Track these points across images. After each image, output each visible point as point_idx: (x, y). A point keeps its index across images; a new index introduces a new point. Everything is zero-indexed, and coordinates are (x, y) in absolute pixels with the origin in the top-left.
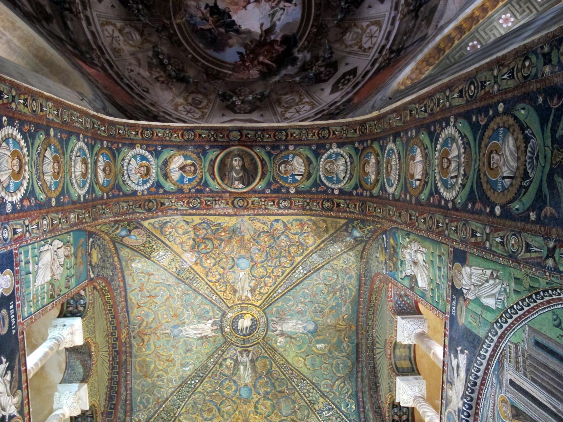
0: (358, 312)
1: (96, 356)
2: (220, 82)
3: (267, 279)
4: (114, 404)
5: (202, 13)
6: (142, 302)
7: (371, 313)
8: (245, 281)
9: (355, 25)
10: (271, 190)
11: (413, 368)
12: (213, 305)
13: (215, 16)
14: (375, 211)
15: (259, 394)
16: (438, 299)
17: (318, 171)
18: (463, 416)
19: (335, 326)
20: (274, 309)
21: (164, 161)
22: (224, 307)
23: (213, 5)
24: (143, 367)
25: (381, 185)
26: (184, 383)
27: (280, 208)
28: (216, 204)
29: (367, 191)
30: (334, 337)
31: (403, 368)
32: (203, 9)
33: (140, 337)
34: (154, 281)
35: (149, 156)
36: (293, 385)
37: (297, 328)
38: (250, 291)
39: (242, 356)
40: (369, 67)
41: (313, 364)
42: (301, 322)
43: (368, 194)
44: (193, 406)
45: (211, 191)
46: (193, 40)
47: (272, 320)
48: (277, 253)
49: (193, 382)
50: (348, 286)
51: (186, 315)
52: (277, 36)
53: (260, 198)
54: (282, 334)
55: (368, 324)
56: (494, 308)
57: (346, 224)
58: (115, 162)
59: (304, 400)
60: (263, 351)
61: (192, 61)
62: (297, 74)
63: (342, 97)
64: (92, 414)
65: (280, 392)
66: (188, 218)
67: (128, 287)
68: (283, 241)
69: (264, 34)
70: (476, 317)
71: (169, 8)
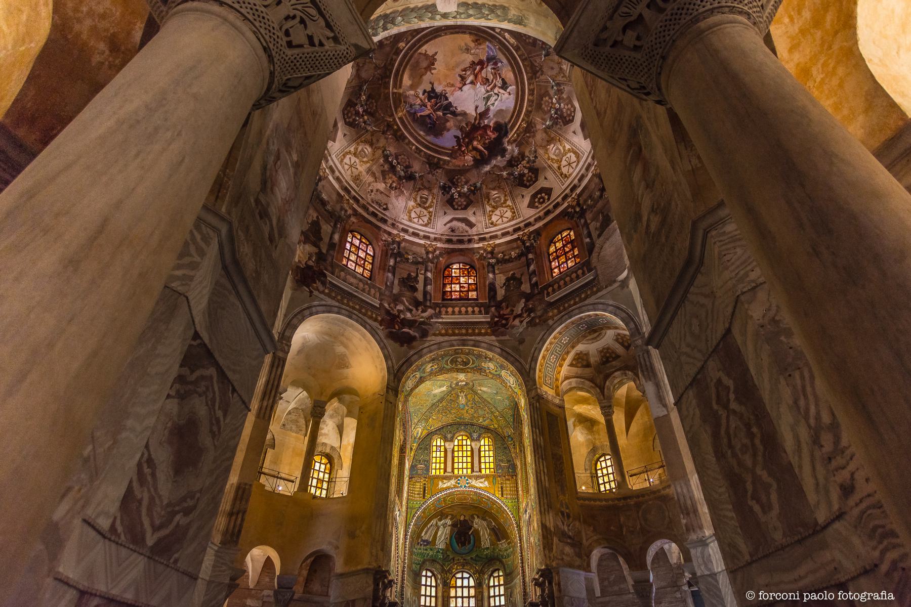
2: (439, 171)
5: (421, 100)
9: (560, 141)
13: (432, 101)
23: (430, 90)
26: (433, 405)
32: (421, 95)
40: (560, 199)
46: (415, 130)
52: (490, 121)
54: (481, 390)
61: (415, 152)
62: (504, 168)
63: (536, 220)
69: (478, 117)
71: (391, 106)
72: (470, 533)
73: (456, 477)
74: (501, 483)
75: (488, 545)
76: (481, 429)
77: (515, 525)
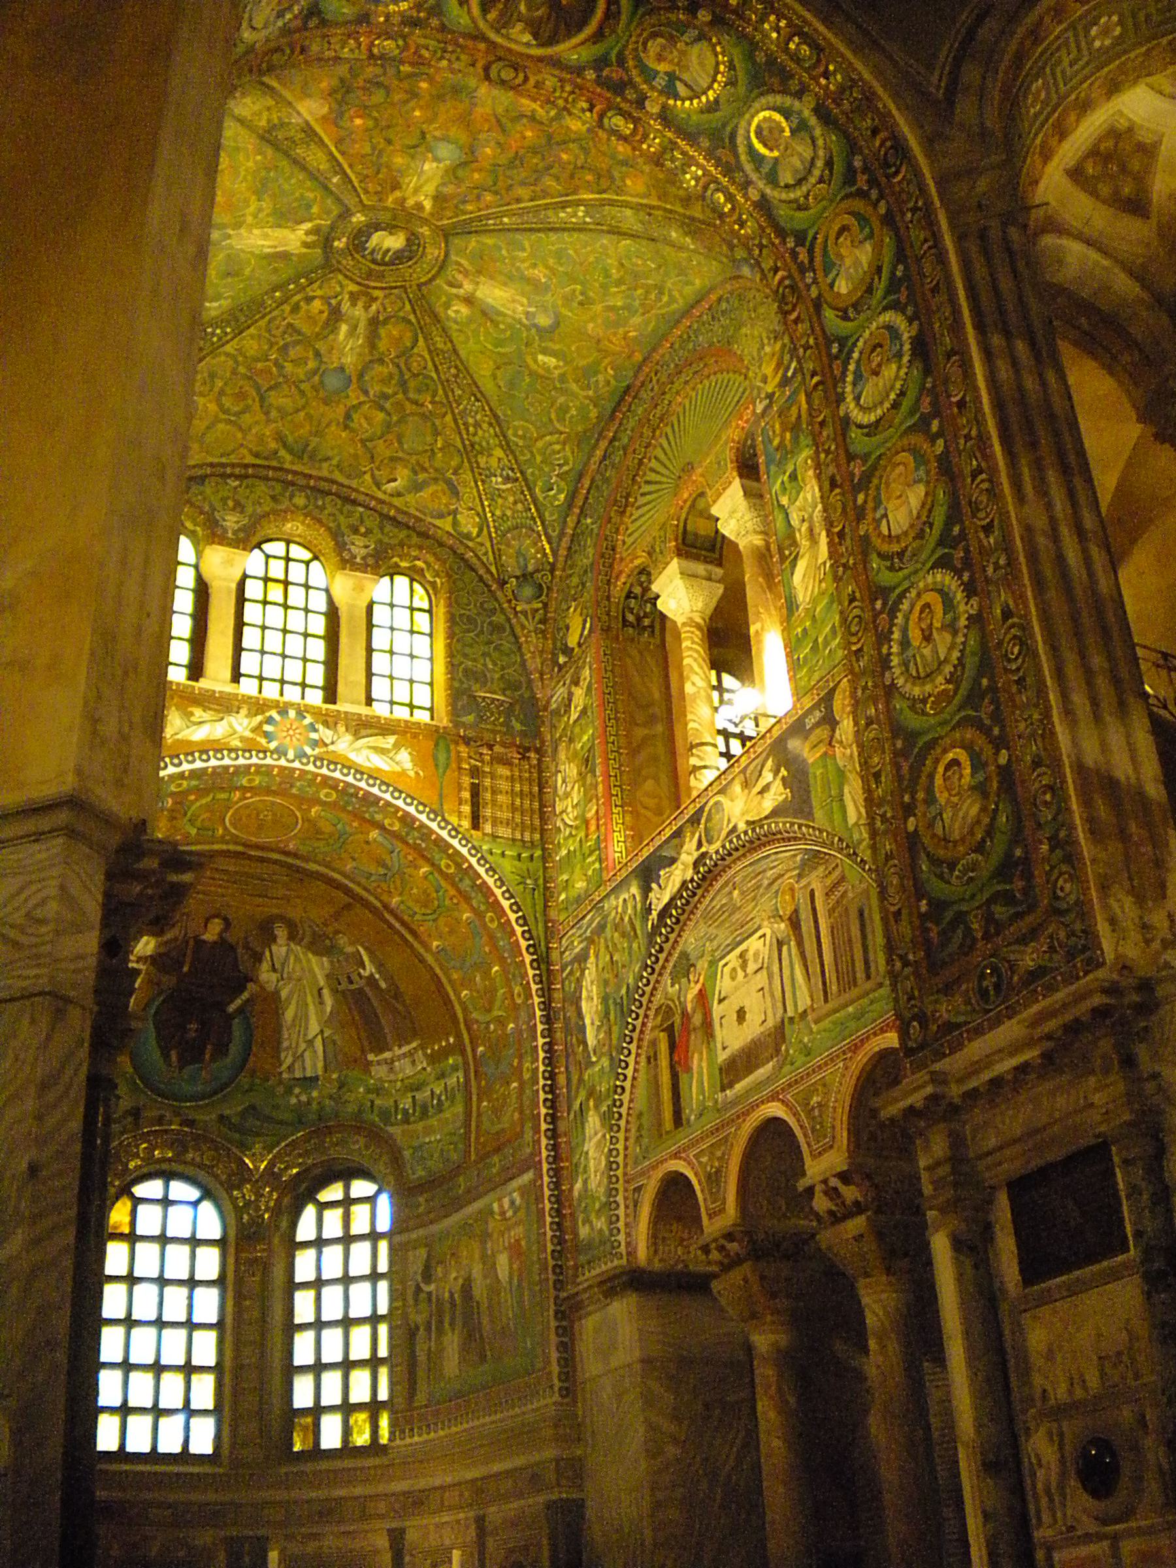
0: (664, 337)
15: (366, 393)
22: (351, 201)
28: (442, 58)
29: (815, 281)
31: (696, 535)
39: (354, 305)
42: (525, 301)
43: (814, 292)
45: (443, 28)
47: (459, 264)
48: (541, 165)
51: (252, 209)
54: (469, 300)
60: (408, 307)
65: (416, 403)
72: (232, 1008)
73: (258, 706)
74: (475, 772)
75: (314, 1064)
76: (388, 528)
77: (528, 958)
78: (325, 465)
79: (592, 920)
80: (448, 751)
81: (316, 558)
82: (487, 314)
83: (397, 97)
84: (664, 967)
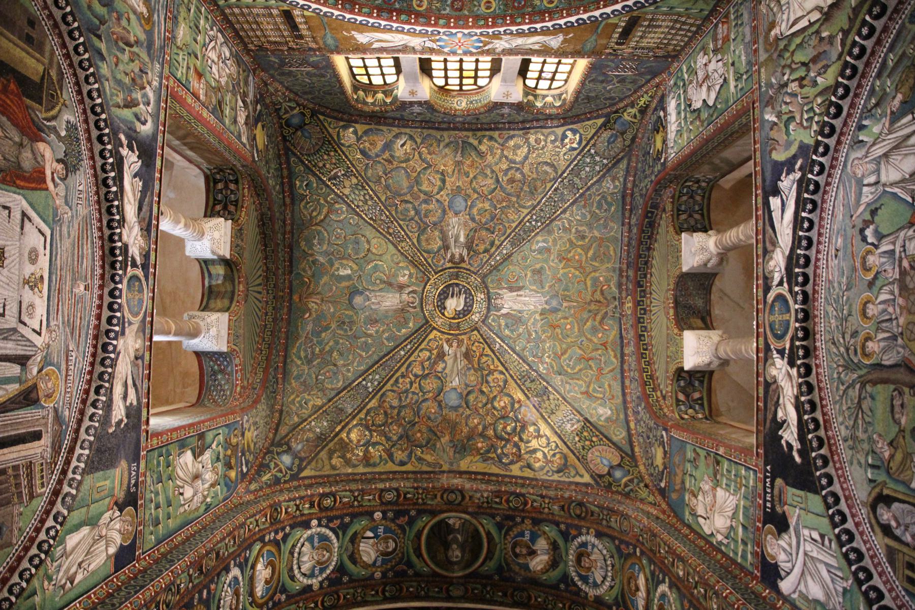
1: (668, 299)
3: (420, 373)
4: (647, 217)
6: (600, 352)
7: (268, 326)
8: (452, 371)
10: (408, 514)
11: (206, 265)
12: (500, 335)
14: (257, 521)
15: (438, 201)
16: (159, 463)
17: (340, 547)
18: (117, 328)
19: (322, 300)
20: (411, 325)
21: (557, 567)
24: (604, 253)
25: (246, 565)
26: (547, 226)
27: (397, 490)
28: (487, 498)
30: (325, 284)
33: (606, 299)
34: (581, 382)
35: (576, 579)
36: (388, 211)
37: (379, 299)
38: (444, 355)
39: (461, 255)
41: (358, 243)
42: (373, 307)
43: (267, 539)
44: (536, 190)
45: (493, 516)
47: (415, 307)
48: (402, 414)
49: (534, 223)
50: (302, 364)
53: (424, 504)
54: (401, 287)
55: (274, 308)
56: (68, 537)
57: (301, 470)
58: (623, 589)
59: (372, 190)
60: (430, 260)
64: (678, 215)
65: (407, 202)
66: (528, 473)
67: (619, 376)
68: (395, 431)
70: (97, 496)
74: (301, 37)
76: (398, 116)
78: (447, 141)
79: (159, 32)
80: (324, 43)
81: (441, 88)
82: (391, 285)
83: (491, 432)
84: (86, 121)
